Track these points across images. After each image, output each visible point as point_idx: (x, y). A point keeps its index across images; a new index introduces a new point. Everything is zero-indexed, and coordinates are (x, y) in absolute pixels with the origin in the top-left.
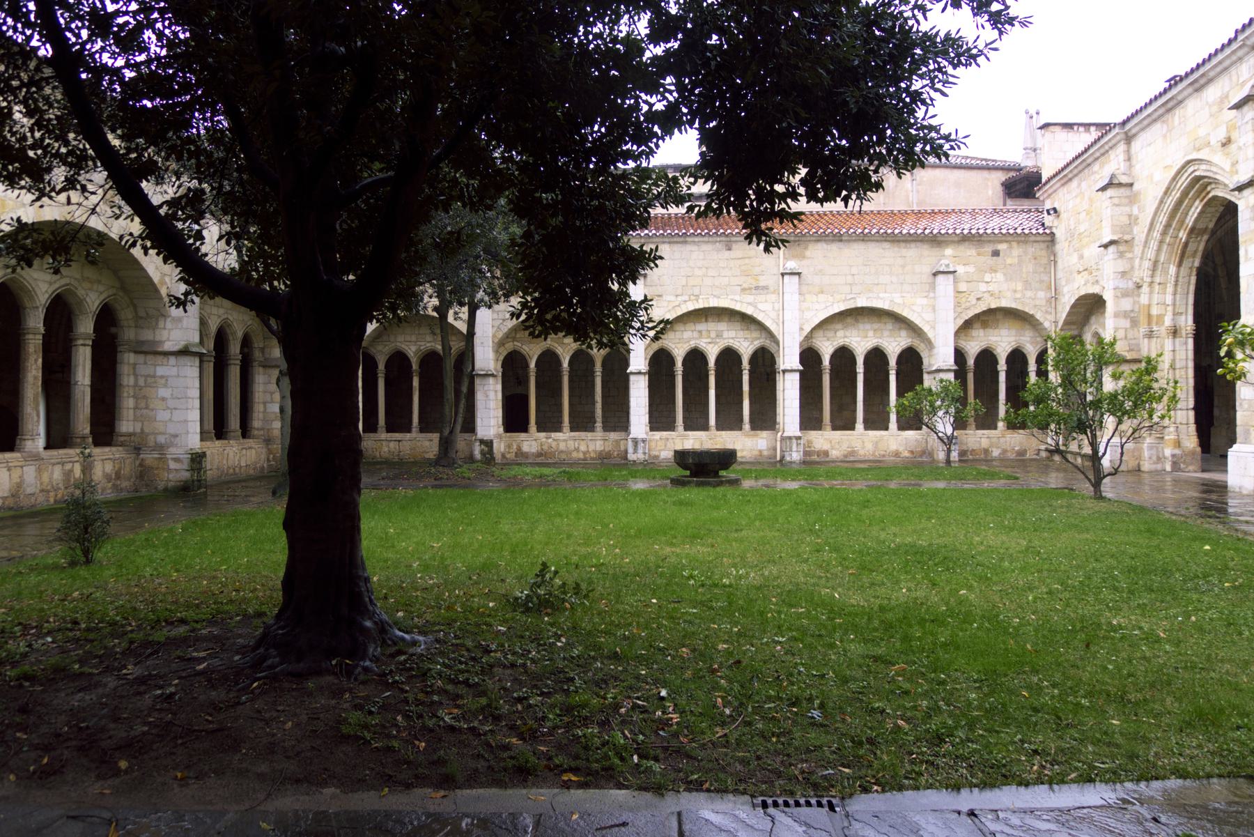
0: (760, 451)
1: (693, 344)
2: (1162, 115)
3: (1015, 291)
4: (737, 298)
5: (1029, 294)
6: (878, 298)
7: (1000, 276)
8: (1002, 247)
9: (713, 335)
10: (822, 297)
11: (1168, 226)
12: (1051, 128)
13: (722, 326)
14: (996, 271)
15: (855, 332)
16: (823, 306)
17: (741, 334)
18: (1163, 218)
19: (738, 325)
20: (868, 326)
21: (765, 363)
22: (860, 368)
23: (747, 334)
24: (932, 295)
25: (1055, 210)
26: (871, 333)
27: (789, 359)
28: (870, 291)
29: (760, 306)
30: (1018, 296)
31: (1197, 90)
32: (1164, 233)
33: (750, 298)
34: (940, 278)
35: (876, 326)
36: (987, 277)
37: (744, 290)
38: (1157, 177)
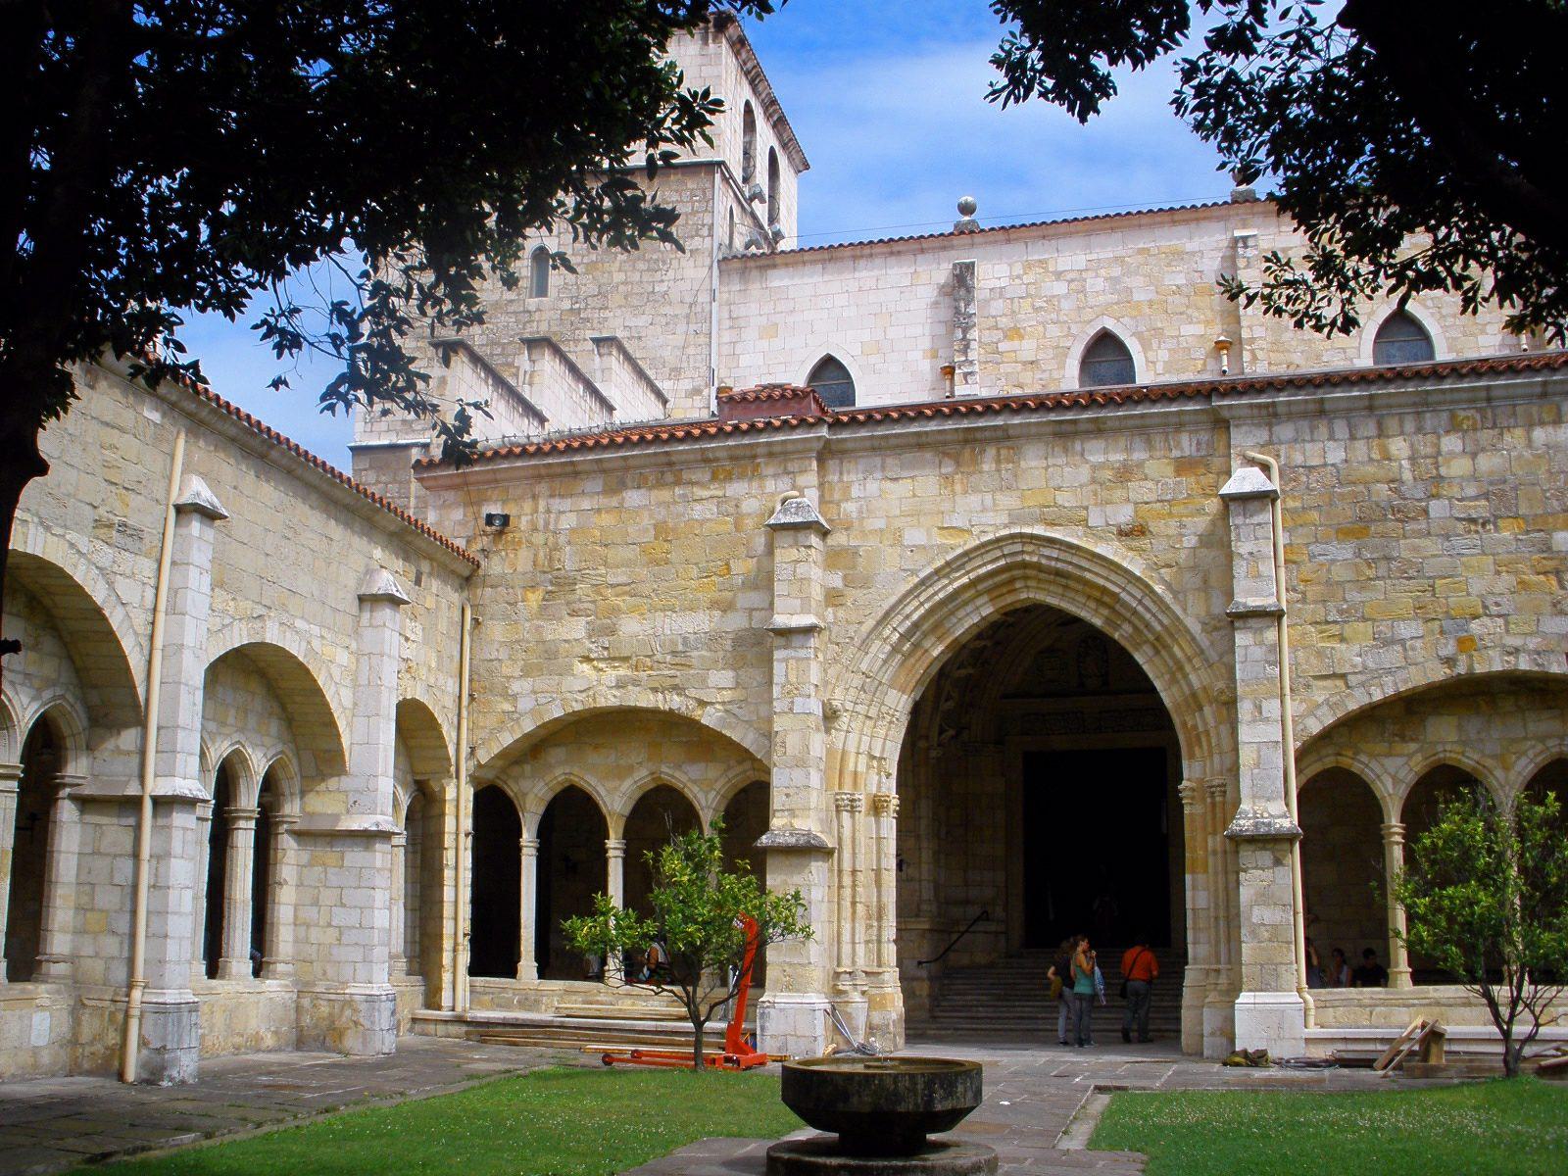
0: (35, 1051)
2: (945, 443)
3: (430, 669)
4: (83, 544)
11: (916, 625)
18: (916, 610)
29: (123, 586)
30: (432, 681)
31: (1055, 435)
32: (904, 637)
33: (106, 555)
34: (386, 613)
37: (98, 523)
38: (915, 536)
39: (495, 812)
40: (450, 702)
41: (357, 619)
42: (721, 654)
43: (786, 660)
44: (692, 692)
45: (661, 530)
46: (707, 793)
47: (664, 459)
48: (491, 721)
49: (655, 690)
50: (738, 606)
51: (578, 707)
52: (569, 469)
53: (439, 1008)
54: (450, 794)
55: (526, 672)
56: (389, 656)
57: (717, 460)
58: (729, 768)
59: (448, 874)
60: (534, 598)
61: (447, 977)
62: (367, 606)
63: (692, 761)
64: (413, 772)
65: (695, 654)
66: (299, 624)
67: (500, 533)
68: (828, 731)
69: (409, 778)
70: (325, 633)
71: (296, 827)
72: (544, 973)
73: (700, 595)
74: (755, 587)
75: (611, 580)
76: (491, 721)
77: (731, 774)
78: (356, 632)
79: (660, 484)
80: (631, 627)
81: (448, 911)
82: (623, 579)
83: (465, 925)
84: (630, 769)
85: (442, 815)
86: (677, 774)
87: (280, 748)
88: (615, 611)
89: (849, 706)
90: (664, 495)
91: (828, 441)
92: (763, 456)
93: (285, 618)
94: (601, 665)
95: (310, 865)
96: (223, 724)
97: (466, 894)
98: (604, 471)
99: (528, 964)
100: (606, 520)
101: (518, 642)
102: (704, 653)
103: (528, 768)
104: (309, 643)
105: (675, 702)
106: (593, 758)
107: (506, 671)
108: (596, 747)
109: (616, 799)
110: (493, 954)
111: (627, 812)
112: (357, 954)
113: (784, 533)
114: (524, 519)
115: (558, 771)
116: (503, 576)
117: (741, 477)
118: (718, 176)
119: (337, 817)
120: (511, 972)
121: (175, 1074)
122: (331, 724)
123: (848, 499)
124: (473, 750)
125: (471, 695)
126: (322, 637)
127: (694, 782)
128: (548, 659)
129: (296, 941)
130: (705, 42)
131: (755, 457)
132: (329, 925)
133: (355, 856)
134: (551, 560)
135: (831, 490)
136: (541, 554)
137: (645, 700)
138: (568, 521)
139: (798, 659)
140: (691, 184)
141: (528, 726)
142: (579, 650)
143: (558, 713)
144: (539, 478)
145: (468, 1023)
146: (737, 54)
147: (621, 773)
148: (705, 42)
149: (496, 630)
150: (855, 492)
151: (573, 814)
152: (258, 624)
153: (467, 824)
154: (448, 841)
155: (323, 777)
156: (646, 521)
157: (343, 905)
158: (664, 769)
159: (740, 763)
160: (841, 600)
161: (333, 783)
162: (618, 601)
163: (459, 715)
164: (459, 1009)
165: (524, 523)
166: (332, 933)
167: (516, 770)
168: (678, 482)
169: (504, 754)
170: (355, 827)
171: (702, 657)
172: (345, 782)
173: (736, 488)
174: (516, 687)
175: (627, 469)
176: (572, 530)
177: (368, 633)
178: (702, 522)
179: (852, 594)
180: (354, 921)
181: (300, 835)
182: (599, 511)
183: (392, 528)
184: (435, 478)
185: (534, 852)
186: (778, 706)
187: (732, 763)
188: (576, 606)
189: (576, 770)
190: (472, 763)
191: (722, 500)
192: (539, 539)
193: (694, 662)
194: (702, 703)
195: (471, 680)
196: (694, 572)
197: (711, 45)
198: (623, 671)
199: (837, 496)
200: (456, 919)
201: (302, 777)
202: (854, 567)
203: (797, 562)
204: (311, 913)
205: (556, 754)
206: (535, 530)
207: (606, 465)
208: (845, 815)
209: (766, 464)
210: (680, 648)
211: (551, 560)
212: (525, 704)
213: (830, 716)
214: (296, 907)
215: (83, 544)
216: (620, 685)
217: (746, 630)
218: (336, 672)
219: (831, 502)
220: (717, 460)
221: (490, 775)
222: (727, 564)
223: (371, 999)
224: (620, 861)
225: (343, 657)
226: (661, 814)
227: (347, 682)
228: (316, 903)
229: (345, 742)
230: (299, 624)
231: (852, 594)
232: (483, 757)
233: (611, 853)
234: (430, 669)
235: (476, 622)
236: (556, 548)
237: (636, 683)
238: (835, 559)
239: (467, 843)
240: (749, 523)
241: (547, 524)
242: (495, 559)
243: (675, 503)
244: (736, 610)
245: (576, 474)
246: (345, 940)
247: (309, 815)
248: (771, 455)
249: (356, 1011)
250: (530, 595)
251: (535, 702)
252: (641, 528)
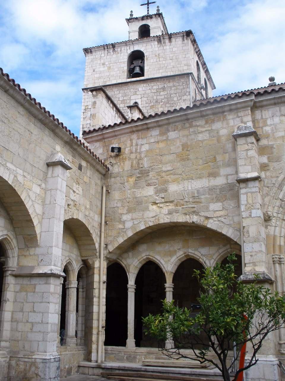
3: (86, 208)
5: (92, 214)
8: (84, 164)
24: (43, 186)
25: (119, 149)
30: (87, 213)
34: (59, 170)
39: (116, 274)
40: (96, 225)
41: (46, 174)
42: (214, 196)
43: (246, 193)
44: (202, 214)
45: (185, 147)
46: (210, 260)
47: (185, 117)
48: (114, 233)
49: (185, 214)
50: (221, 174)
51: (151, 224)
52: (145, 127)
53: (90, 361)
54: (97, 265)
55: (129, 211)
56: (61, 191)
57: (207, 115)
58: (220, 248)
59: (95, 300)
60: (132, 180)
61: (94, 346)
62: (51, 169)
63: (203, 246)
64: (81, 256)
65: (203, 197)
66: (9, 165)
67: (117, 156)
68: (266, 227)
69: (79, 259)
70: (26, 174)
71: (14, 273)
72: (138, 344)
73: (203, 172)
74: (229, 165)
75: (164, 169)
76: (114, 233)
77: (220, 251)
78: (45, 179)
79: (183, 128)
80: (173, 188)
81: (95, 316)
82: (169, 168)
83: (103, 322)
84: (175, 252)
85: (93, 274)
86: (196, 253)
87: (5, 232)
88: (166, 182)
89: (275, 215)
90: (186, 132)
91: (255, 102)
92: (227, 111)
94: (161, 205)
95: (20, 291)
97: (103, 309)
98: (159, 126)
99: (131, 340)
100: (161, 145)
101: (125, 199)
102: (207, 196)
103: (130, 254)
104: (15, 176)
105: (195, 219)
106: (159, 248)
107: (120, 211)
108: (160, 243)
109: (169, 265)
110: (115, 335)
111: (174, 272)
112: (39, 337)
113: (241, 138)
114: (127, 149)
115: (143, 255)
116: (119, 173)
117: (219, 120)
118: (190, 77)
119: (33, 268)
120: (124, 344)
122: (31, 221)
123: (266, 125)
124: (106, 245)
125: (106, 222)
126: (24, 176)
127: (204, 256)
128: (138, 205)
129: (12, 330)
130: (183, 40)
131: (224, 112)
132: (27, 322)
133: (40, 286)
134: (138, 164)
135: (258, 122)
136: (134, 162)
137: (180, 218)
138: (146, 148)
139: (252, 193)
140: (182, 80)
141: (130, 234)
142: (152, 200)
143: (142, 227)
144: (133, 132)
145: (103, 369)
146: (193, 45)
147: (171, 254)
148: (183, 40)
149: (116, 195)
150: (269, 122)
151: (150, 272)
153: (104, 278)
154: (96, 285)
155: (27, 247)
156: (178, 144)
157: (34, 312)
158: (190, 251)
159: (224, 246)
160: (267, 168)
161: (32, 251)
162: (168, 178)
163: (101, 231)
164: (99, 361)
165: (127, 151)
166: (29, 326)
167: (125, 255)
168: (191, 126)
169: (119, 248)
170: (41, 272)
171: (206, 198)
172: (38, 251)
173: (217, 125)
174: (124, 218)
175: (169, 124)
176: (147, 151)
177: (50, 181)
178: (202, 141)
179: (272, 165)
180: (39, 320)
181: (16, 276)
182: (158, 142)
183: (66, 138)
184: (91, 137)
185: (134, 290)
186: (244, 215)
187: (221, 246)
188: (149, 182)
189: (151, 254)
190: (106, 252)
191: (210, 131)
192: (133, 156)
193: (203, 200)
194: (207, 218)
195: (105, 217)
196: (201, 162)
197: (185, 41)
198: (171, 207)
199: (261, 125)
200: (98, 320)
201: (19, 249)
202: (272, 153)
203: (247, 150)
204: (19, 316)
205: (143, 248)
206: (132, 153)
207: (160, 123)
208: (277, 265)
209: (229, 115)
210: (196, 195)
211: (138, 164)
212: (129, 225)
213: (267, 219)
214: (13, 312)
216: (170, 213)
217: (225, 184)
218: (33, 196)
219: (259, 127)
220: (207, 115)
221: (114, 257)
222: (215, 157)
223: (45, 361)
224: (171, 293)
225: (37, 189)
226: (189, 268)
227: (40, 202)
228: (22, 311)
229: (38, 230)
230: (9, 165)
231: (272, 165)
232: (111, 248)
233: (167, 289)
234: (86, 208)
235: (108, 192)
236: (141, 159)
237: (177, 212)
238: (262, 151)
239: (104, 287)
240: (223, 139)
241: (136, 150)
242: (116, 166)
243: (190, 135)
244: (221, 176)
245: (148, 129)
246: (34, 330)
247: (20, 267)
248: (231, 110)
249: (37, 368)
250: (130, 180)
251: (132, 224)
252: (176, 147)
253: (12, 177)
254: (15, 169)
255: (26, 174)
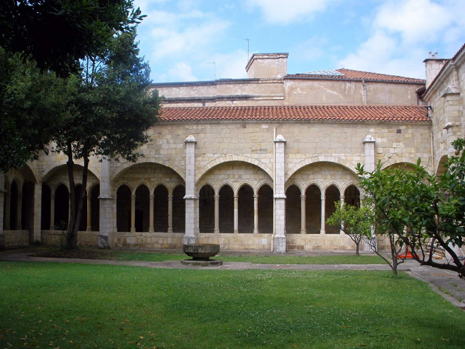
0: (264, 245)
1: (224, 182)
3: (411, 153)
6: (331, 156)
7: (402, 145)
8: (402, 128)
9: (236, 177)
10: (298, 156)
12: (430, 62)
13: (242, 172)
14: (399, 142)
15: (320, 176)
16: (299, 161)
17: (253, 176)
19: (251, 172)
20: (327, 173)
21: (267, 192)
22: (323, 197)
23: (256, 176)
24: (362, 155)
26: (329, 177)
27: (279, 192)
28: (327, 152)
30: (412, 156)
33: (257, 156)
34: (367, 145)
35: (332, 172)
36: (395, 145)
37: (253, 151)
66: (333, 155)
70: (346, 154)
87: (352, 181)
93: (327, 154)
96: (326, 179)
121: (277, 250)
152: (316, 158)
215: (249, 155)
230: (333, 155)
253: (337, 159)
254: (338, 155)
255: (346, 154)
